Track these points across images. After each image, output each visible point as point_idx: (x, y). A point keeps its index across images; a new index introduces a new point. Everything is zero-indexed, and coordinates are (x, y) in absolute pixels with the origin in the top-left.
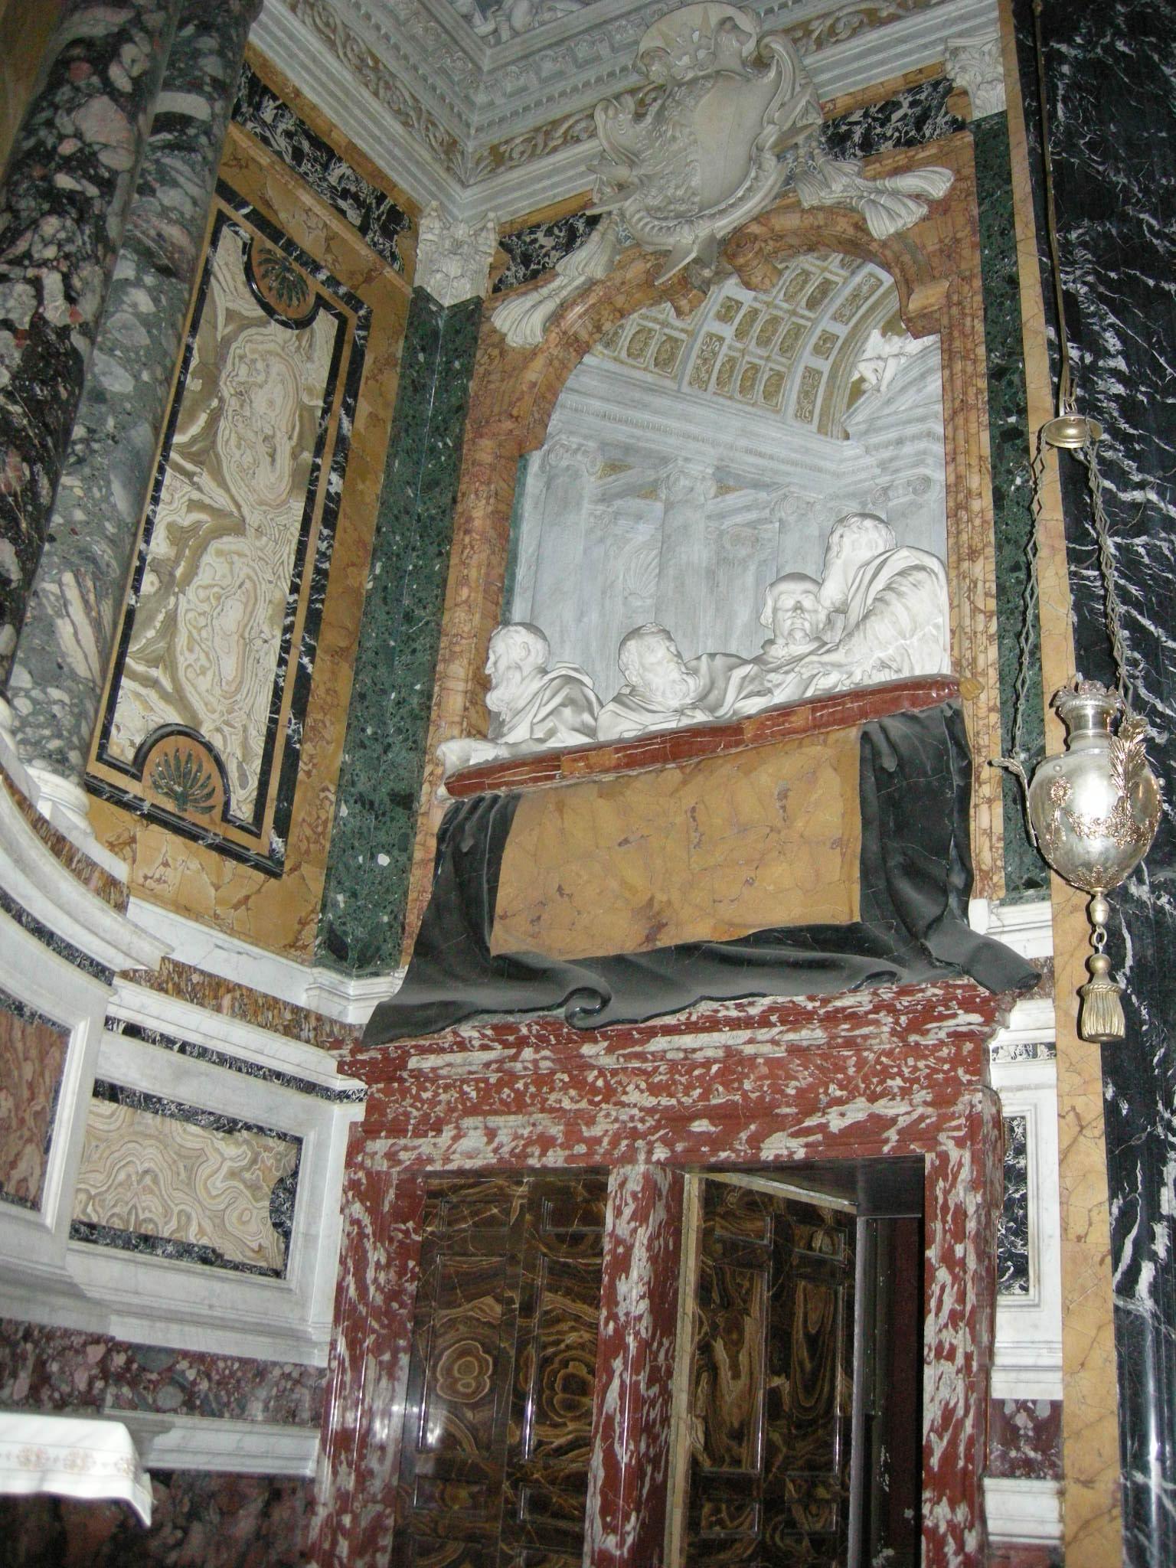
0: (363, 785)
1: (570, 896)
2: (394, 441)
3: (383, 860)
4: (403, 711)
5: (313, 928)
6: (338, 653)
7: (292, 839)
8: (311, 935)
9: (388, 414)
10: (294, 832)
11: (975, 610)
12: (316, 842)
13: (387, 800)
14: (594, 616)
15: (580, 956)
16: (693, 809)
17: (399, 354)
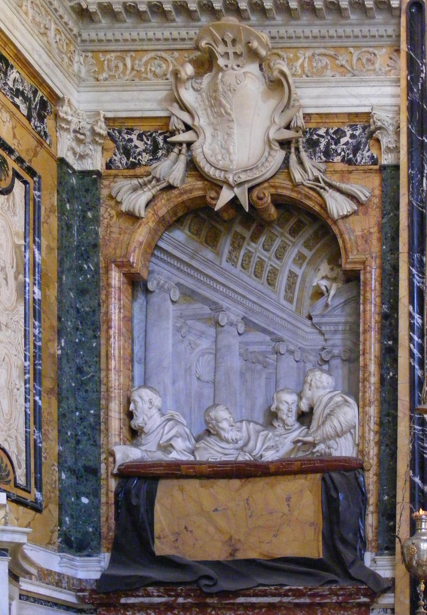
0: (70, 462)
1: (191, 532)
2: (61, 262)
3: (85, 500)
4: (85, 423)
5: (56, 534)
6: (50, 392)
7: (44, 492)
8: (57, 540)
9: (54, 244)
10: (45, 488)
11: (370, 430)
12: (53, 492)
13: (82, 470)
14: (181, 383)
15: (199, 559)
16: (247, 500)
17: (56, 204)
